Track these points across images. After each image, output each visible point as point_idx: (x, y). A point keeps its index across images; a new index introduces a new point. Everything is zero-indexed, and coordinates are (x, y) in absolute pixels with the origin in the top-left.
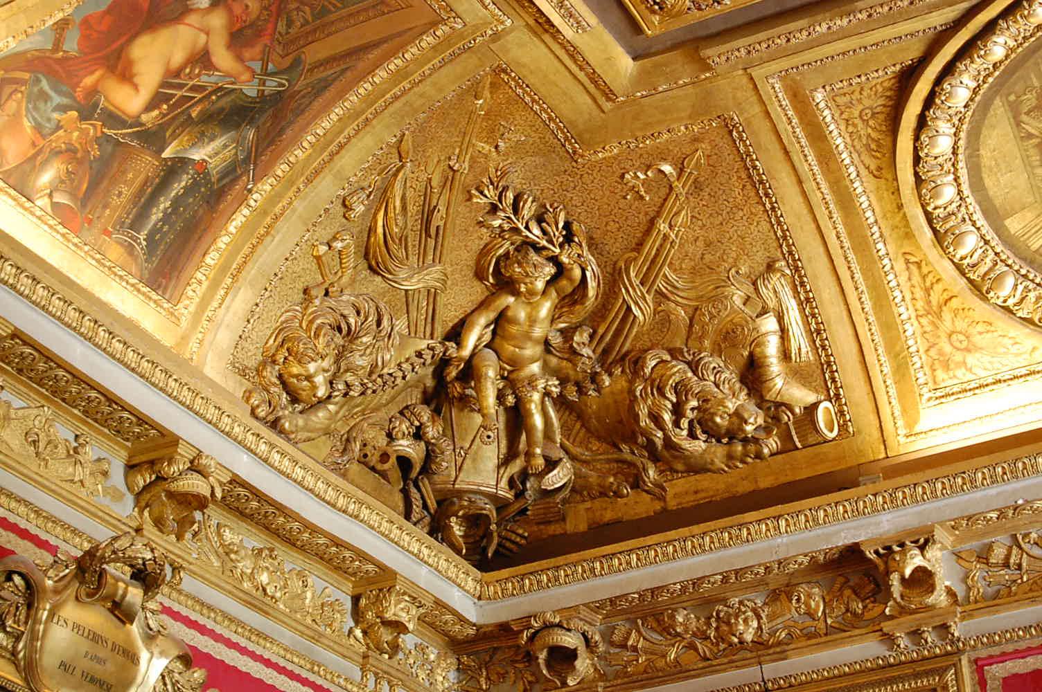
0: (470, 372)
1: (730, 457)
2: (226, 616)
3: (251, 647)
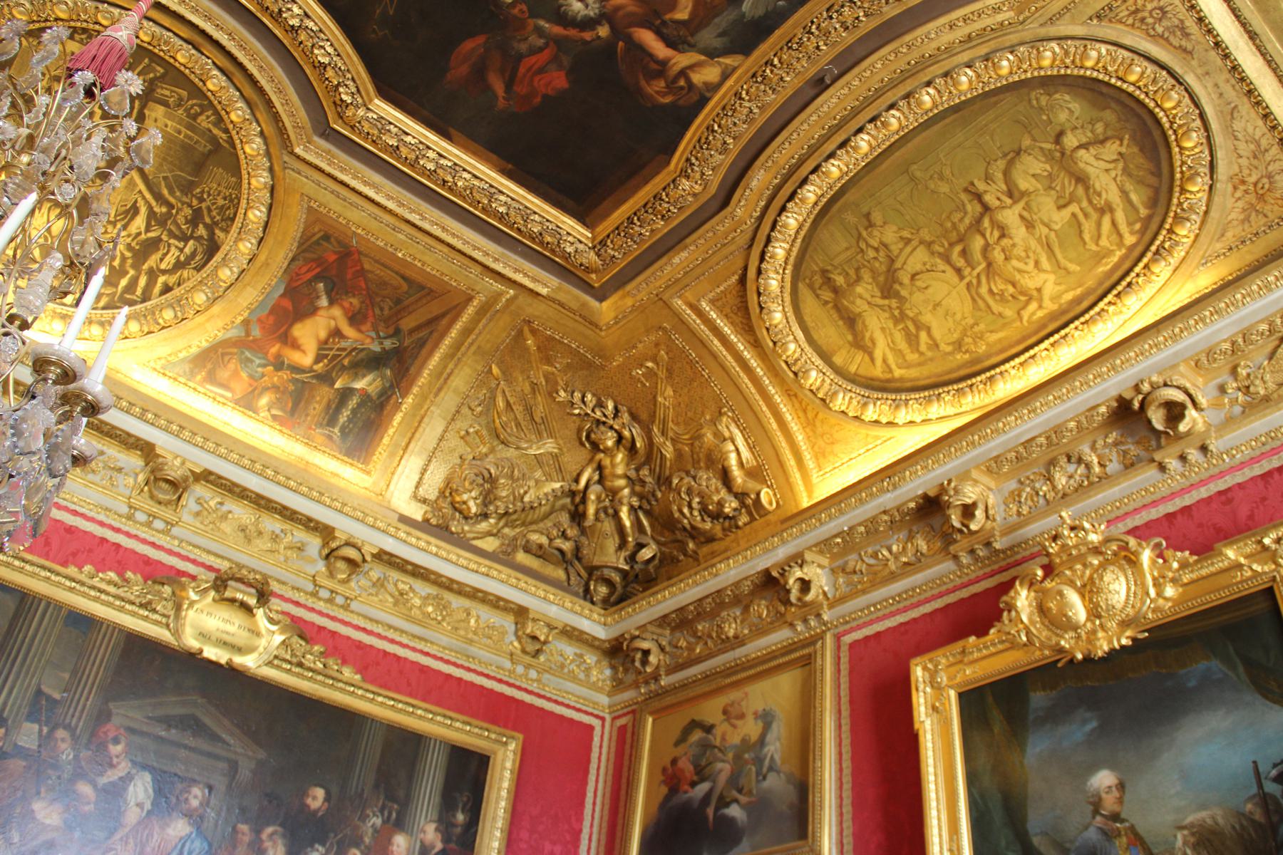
1: (724, 530)
2: (390, 627)
3: (412, 644)
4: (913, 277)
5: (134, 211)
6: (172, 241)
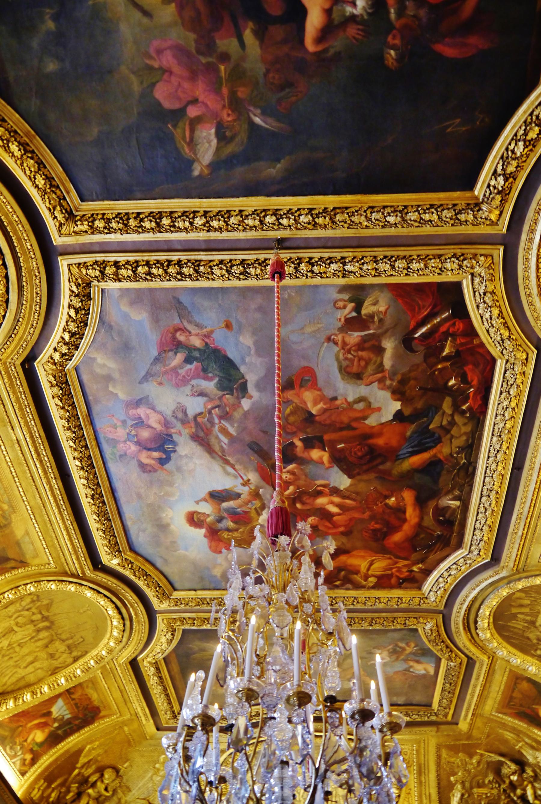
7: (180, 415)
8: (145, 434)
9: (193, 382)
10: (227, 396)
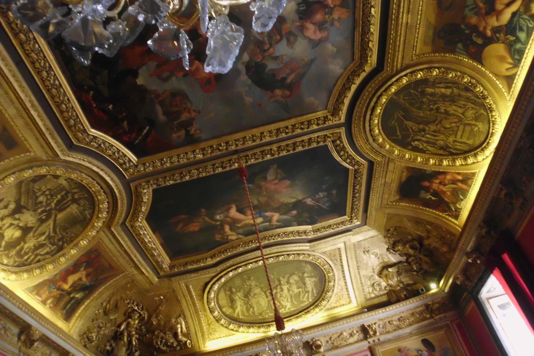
0: (122, 333)
4: (255, 294)
5: (44, 233)
6: (50, 245)
7: (292, 38)
8: (319, 17)
9: (282, 65)
10: (259, 60)
